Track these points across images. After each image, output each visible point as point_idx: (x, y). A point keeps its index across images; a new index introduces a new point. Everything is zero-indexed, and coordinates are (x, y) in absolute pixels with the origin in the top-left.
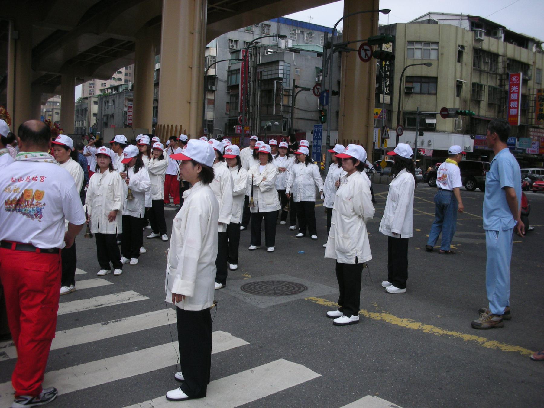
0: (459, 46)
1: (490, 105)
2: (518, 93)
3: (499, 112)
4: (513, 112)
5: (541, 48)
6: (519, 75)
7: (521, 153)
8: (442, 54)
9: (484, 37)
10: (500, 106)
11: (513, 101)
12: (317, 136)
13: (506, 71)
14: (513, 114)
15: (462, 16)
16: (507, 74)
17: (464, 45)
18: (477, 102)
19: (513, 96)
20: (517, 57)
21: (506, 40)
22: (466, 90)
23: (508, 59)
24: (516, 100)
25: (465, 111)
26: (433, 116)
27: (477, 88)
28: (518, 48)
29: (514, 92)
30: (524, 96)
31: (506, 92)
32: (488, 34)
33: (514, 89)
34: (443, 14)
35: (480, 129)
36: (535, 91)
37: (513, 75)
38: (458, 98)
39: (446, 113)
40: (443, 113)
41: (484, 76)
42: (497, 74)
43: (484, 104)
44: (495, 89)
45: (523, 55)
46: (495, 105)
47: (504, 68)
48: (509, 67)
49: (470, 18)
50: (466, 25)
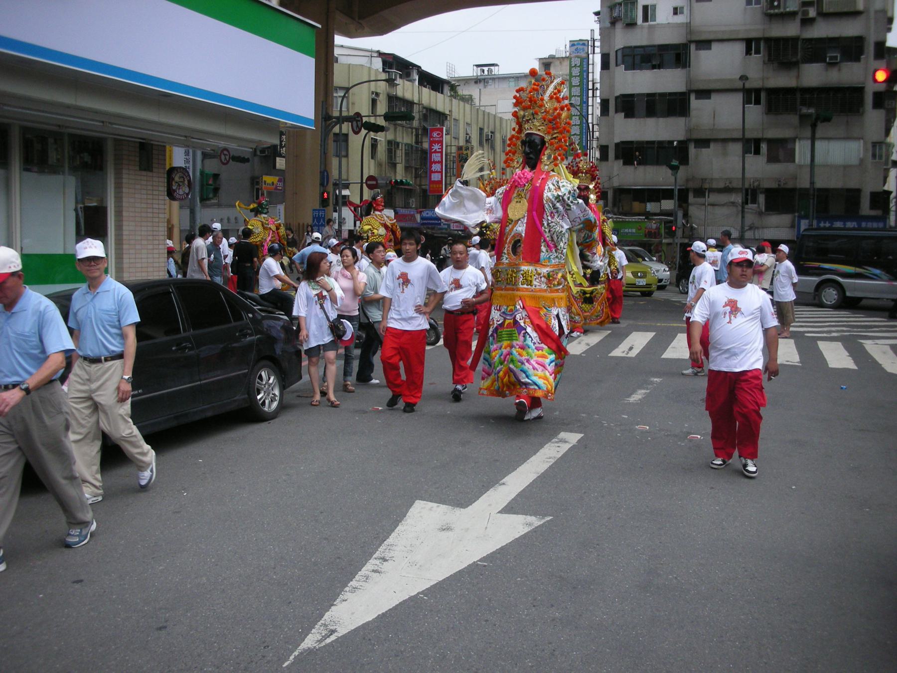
0: (373, 93)
1: (407, 168)
2: (441, 153)
3: (416, 178)
4: (435, 177)
5: (456, 92)
6: (442, 130)
7: (446, 229)
8: (353, 104)
9: (399, 81)
10: (416, 169)
11: (436, 163)
12: (319, 221)
13: (423, 123)
14: (436, 179)
15: (371, 51)
16: (425, 130)
17: (378, 91)
18: (394, 165)
19: (436, 157)
20: (434, 107)
21: (420, 83)
22: (382, 149)
23: (424, 108)
24: (438, 162)
25: (401, 181)
26: (347, 186)
27: (392, 146)
28: (433, 93)
29: (436, 152)
30: (446, 155)
31: (424, 152)
32: (401, 77)
33: (436, 147)
34: (342, 46)
35: (399, 200)
36: (454, 149)
37: (432, 131)
38: (372, 161)
39: (374, 183)
40: (369, 182)
41: (399, 129)
42: (412, 128)
43: (400, 168)
44: (412, 146)
45: (439, 101)
46: (412, 167)
47: (419, 119)
48: (425, 117)
49: (380, 54)
50: (378, 64)
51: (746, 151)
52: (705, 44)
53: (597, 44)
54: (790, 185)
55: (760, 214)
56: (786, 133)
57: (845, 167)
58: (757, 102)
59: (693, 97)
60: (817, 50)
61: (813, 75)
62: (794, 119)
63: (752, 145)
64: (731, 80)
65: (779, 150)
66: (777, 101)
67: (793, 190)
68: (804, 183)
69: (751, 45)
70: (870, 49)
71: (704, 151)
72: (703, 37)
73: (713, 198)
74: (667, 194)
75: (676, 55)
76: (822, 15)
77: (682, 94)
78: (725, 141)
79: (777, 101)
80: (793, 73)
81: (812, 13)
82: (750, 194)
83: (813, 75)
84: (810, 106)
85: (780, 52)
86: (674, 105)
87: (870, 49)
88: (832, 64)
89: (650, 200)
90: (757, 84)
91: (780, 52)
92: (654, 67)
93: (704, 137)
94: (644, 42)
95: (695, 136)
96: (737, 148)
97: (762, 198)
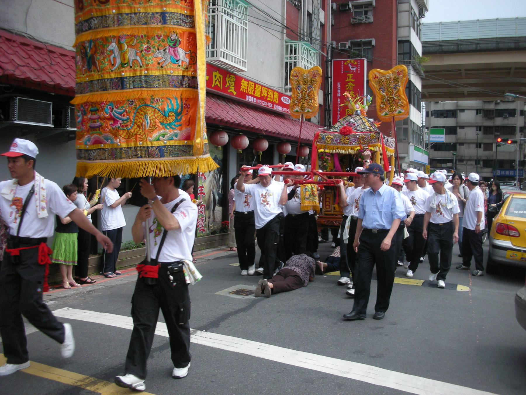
51: (477, 147)
52: (463, 110)
53: (424, 108)
54: (491, 158)
55: (481, 168)
56: (490, 141)
57: (510, 152)
58: (480, 130)
59: (458, 128)
60: (500, 113)
61: (499, 121)
62: (492, 136)
63: (479, 145)
64: (472, 123)
65: (488, 147)
66: (487, 130)
67: (492, 160)
68: (494, 158)
69: (478, 111)
70: (518, 113)
71: (462, 147)
72: (462, 108)
73: (465, 162)
74: (450, 161)
75: (452, 113)
76: (502, 101)
77: (454, 127)
78: (469, 143)
79: (487, 130)
80: (492, 121)
81: (499, 101)
82: (477, 162)
83: (499, 121)
84: (498, 132)
85: (488, 114)
86: (451, 131)
87: (518, 113)
88: (505, 118)
89: (443, 163)
90: (480, 125)
91: (488, 114)
92: (445, 117)
93: (462, 141)
94: (441, 109)
95: (459, 141)
96: (474, 146)
97: (481, 163)
